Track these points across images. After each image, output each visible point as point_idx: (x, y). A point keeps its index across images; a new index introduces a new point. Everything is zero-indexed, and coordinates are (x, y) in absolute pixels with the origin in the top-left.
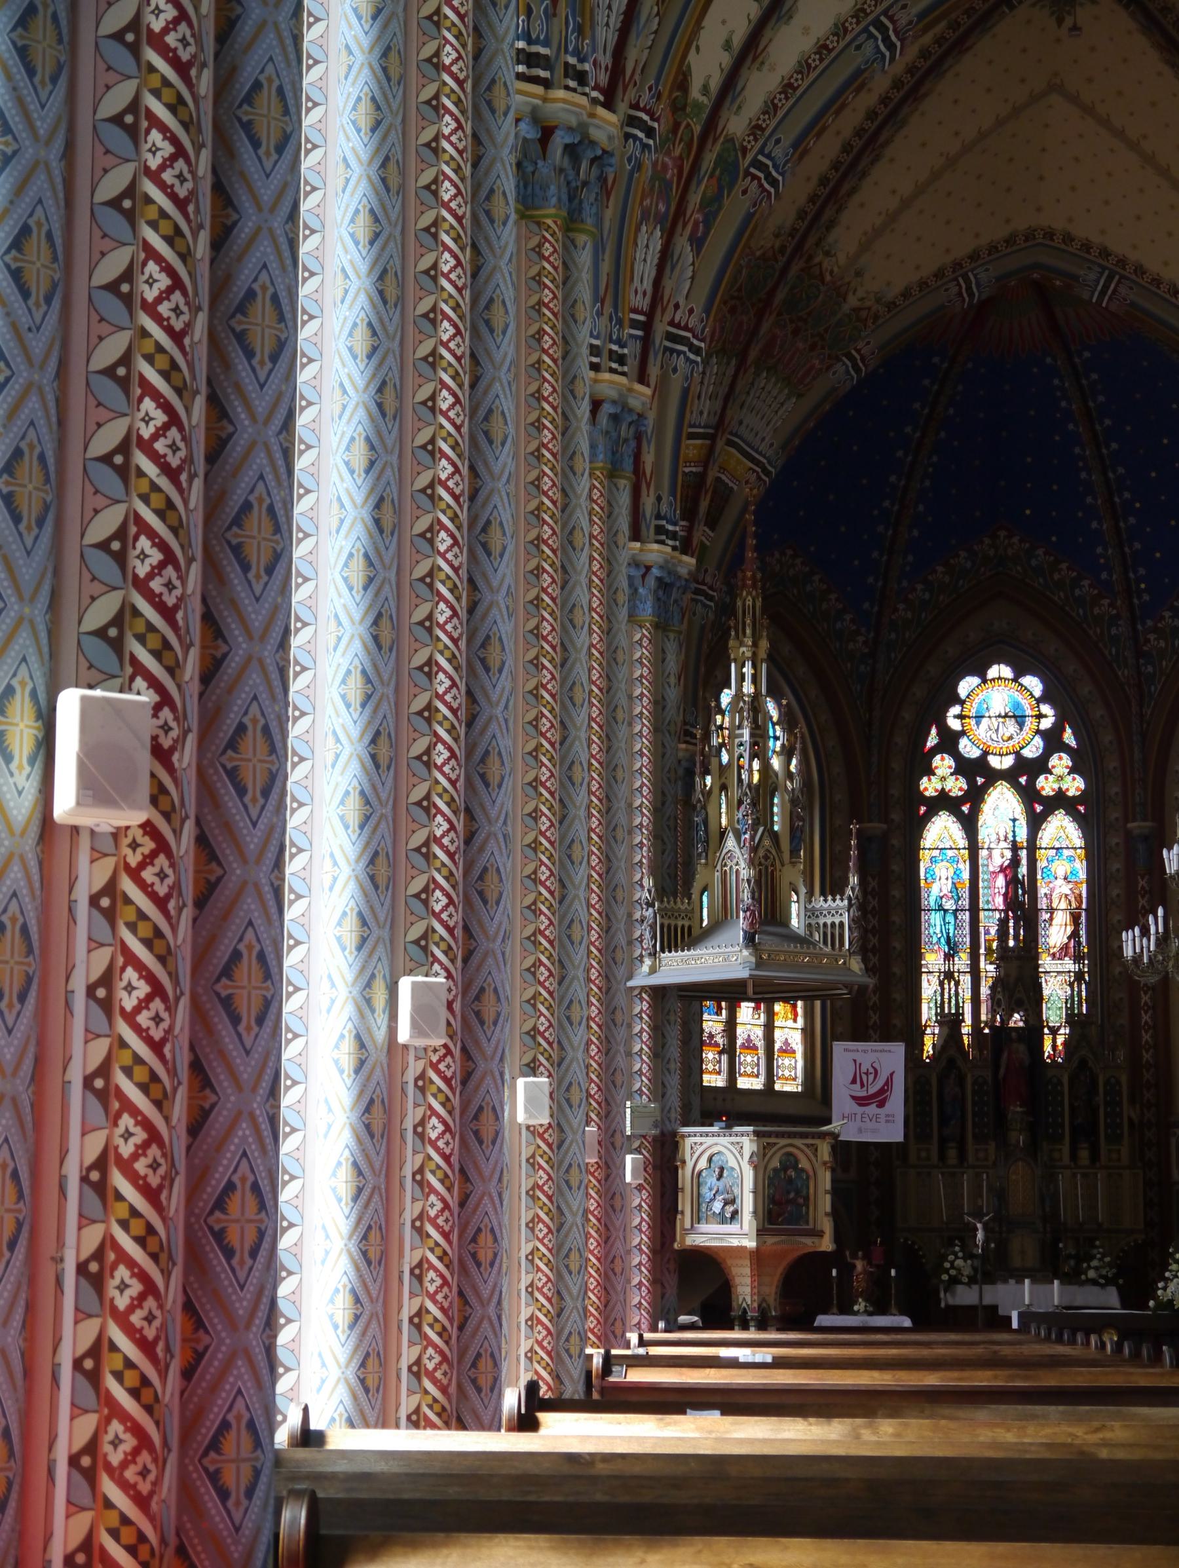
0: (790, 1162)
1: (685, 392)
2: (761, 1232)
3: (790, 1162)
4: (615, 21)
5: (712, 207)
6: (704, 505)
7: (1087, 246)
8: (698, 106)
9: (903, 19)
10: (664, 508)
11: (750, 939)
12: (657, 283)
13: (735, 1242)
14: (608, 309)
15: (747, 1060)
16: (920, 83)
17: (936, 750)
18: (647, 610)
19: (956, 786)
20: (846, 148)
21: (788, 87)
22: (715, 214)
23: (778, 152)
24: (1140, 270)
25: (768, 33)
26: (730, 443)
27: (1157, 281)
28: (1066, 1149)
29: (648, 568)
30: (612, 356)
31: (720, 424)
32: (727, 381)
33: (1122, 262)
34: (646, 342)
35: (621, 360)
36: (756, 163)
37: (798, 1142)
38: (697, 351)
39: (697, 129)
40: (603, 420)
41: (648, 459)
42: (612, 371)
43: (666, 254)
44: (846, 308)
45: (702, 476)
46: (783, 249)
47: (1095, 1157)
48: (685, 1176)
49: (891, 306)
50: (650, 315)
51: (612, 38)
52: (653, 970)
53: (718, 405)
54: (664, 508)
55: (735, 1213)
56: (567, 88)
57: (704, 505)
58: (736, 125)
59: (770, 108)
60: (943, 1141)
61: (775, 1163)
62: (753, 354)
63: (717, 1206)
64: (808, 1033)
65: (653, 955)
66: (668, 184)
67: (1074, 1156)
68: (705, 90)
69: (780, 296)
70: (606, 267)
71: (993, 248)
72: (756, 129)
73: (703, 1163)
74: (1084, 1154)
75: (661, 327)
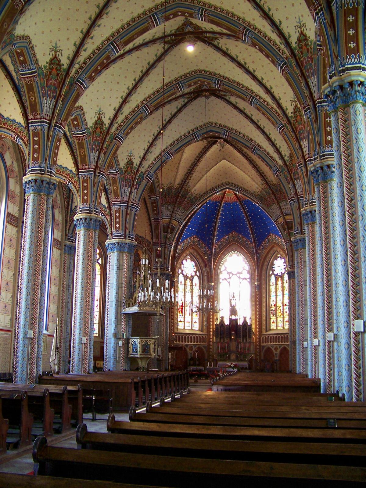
0: (146, 343)
1: (135, 214)
2: (140, 355)
3: (146, 343)
4: (96, 158)
5: (139, 184)
6: (169, 230)
7: (235, 185)
8: (135, 167)
9: (172, 151)
10: (131, 234)
11: (139, 306)
12: (129, 196)
13: (137, 356)
14: (94, 204)
15: (187, 324)
16: (199, 159)
17: (225, 270)
18: (126, 251)
19: (227, 276)
20: (189, 170)
21: (152, 163)
22: (140, 185)
23: (151, 174)
24: (244, 188)
25: (146, 155)
26: (173, 219)
27: (247, 190)
28: (241, 339)
29: (126, 244)
30: (95, 211)
31: (171, 217)
32: (172, 209)
33: (241, 187)
34: (127, 206)
35: (97, 212)
36: (147, 176)
37: (148, 340)
38: (138, 207)
39: (135, 171)
40: (92, 222)
41: (127, 225)
42: (95, 214)
43: (131, 192)
44: (193, 196)
45: (169, 225)
46: (180, 187)
47: (246, 341)
48: (130, 345)
49: (202, 195)
50: (128, 202)
51: (96, 161)
52: (125, 311)
53: (171, 213)
54: (131, 234)
55: (137, 351)
56: (47, 175)
57: (169, 230)
58: (142, 170)
59: (149, 167)
60: (220, 338)
61: (144, 343)
62: (177, 204)
63: (134, 350)
64: (199, 319)
65: (125, 308)
66: (131, 180)
67: (243, 341)
68: (136, 165)
69: (180, 195)
70: (94, 197)
71: (219, 185)
72: (147, 170)
73: (133, 343)
74: (245, 340)
75: (130, 203)
